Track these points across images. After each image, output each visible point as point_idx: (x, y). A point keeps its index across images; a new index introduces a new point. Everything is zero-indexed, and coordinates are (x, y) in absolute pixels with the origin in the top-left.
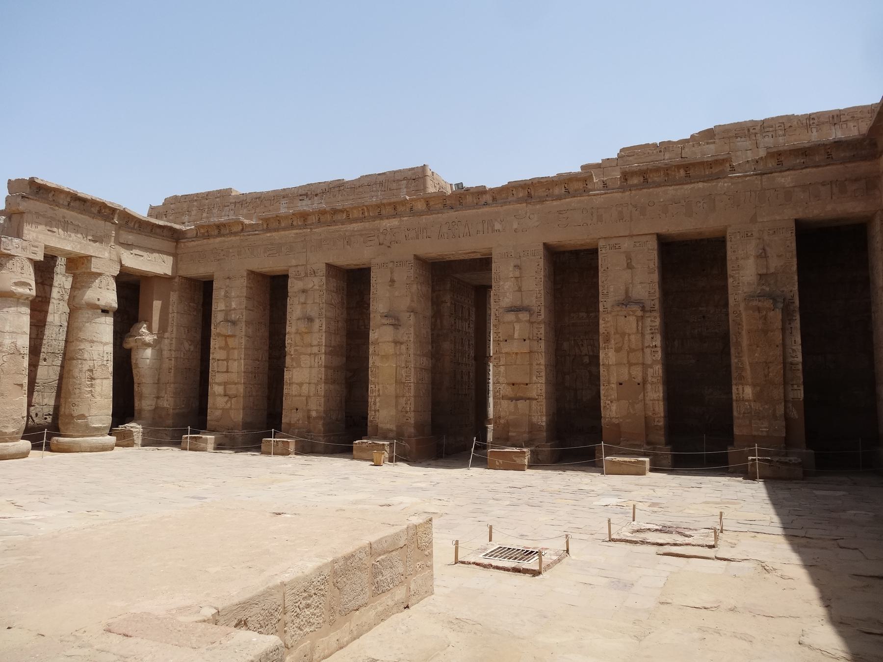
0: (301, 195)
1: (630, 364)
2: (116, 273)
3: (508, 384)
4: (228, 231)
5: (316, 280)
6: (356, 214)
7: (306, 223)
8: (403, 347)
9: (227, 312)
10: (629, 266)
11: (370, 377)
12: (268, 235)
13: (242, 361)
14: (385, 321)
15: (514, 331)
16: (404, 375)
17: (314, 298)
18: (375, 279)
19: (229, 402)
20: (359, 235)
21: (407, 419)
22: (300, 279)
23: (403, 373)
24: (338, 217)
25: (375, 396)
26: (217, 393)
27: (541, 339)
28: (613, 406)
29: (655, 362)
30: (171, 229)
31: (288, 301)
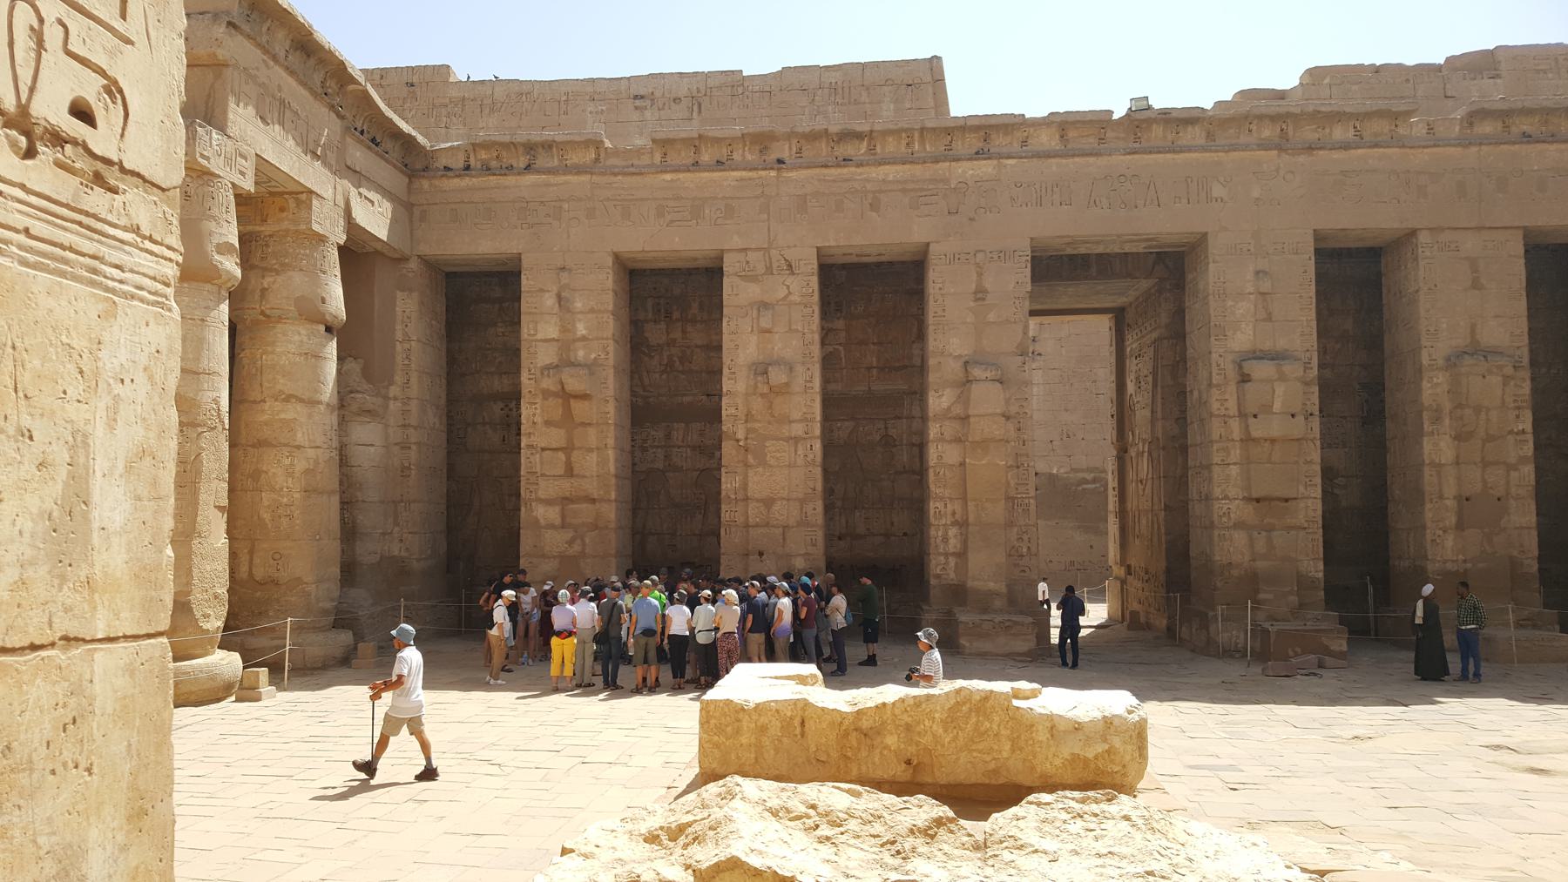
0: (636, 97)
1: (1485, 464)
2: (342, 239)
3: (1248, 499)
4: (556, 160)
5: (795, 283)
6: (891, 146)
7: (766, 158)
8: (1011, 426)
9: (565, 343)
10: (1476, 285)
11: (932, 487)
12: (668, 177)
13: (611, 453)
14: (977, 372)
15: (1273, 397)
16: (1012, 483)
17: (790, 320)
18: (941, 285)
19: (579, 541)
20: (900, 190)
21: (1024, 571)
22: (753, 279)
23: (1009, 477)
24: (848, 149)
25: (944, 525)
26: (542, 522)
27: (1311, 415)
28: (1447, 540)
29: (1523, 460)
30: (408, 142)
31: (725, 324)
